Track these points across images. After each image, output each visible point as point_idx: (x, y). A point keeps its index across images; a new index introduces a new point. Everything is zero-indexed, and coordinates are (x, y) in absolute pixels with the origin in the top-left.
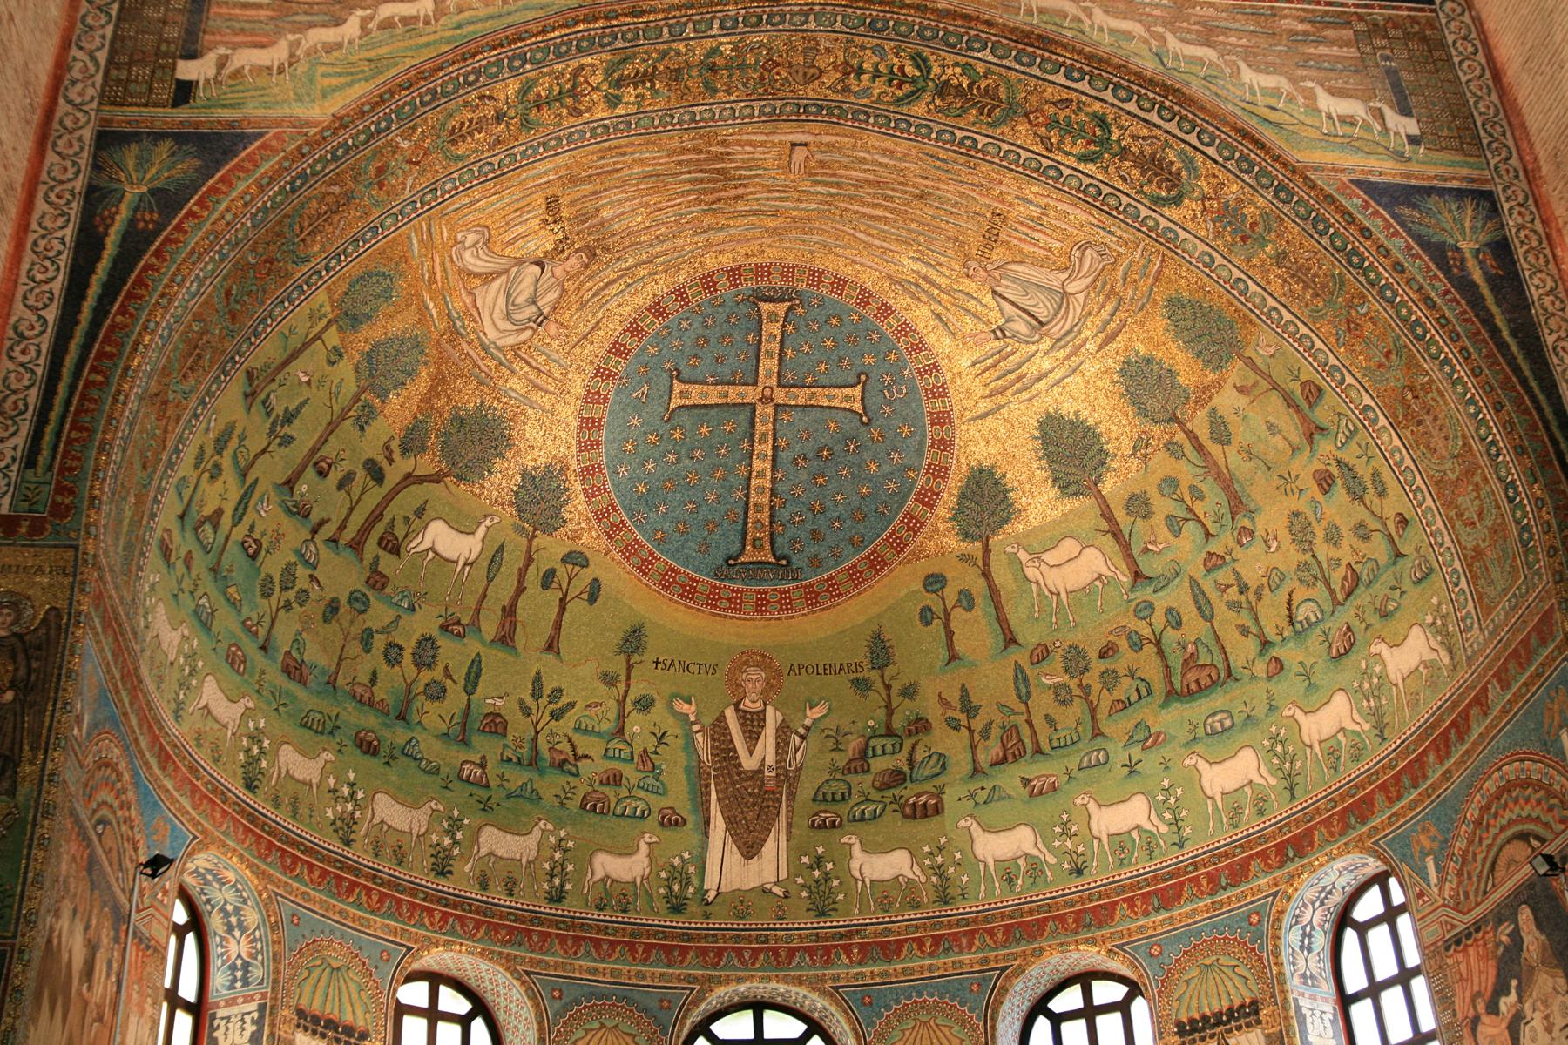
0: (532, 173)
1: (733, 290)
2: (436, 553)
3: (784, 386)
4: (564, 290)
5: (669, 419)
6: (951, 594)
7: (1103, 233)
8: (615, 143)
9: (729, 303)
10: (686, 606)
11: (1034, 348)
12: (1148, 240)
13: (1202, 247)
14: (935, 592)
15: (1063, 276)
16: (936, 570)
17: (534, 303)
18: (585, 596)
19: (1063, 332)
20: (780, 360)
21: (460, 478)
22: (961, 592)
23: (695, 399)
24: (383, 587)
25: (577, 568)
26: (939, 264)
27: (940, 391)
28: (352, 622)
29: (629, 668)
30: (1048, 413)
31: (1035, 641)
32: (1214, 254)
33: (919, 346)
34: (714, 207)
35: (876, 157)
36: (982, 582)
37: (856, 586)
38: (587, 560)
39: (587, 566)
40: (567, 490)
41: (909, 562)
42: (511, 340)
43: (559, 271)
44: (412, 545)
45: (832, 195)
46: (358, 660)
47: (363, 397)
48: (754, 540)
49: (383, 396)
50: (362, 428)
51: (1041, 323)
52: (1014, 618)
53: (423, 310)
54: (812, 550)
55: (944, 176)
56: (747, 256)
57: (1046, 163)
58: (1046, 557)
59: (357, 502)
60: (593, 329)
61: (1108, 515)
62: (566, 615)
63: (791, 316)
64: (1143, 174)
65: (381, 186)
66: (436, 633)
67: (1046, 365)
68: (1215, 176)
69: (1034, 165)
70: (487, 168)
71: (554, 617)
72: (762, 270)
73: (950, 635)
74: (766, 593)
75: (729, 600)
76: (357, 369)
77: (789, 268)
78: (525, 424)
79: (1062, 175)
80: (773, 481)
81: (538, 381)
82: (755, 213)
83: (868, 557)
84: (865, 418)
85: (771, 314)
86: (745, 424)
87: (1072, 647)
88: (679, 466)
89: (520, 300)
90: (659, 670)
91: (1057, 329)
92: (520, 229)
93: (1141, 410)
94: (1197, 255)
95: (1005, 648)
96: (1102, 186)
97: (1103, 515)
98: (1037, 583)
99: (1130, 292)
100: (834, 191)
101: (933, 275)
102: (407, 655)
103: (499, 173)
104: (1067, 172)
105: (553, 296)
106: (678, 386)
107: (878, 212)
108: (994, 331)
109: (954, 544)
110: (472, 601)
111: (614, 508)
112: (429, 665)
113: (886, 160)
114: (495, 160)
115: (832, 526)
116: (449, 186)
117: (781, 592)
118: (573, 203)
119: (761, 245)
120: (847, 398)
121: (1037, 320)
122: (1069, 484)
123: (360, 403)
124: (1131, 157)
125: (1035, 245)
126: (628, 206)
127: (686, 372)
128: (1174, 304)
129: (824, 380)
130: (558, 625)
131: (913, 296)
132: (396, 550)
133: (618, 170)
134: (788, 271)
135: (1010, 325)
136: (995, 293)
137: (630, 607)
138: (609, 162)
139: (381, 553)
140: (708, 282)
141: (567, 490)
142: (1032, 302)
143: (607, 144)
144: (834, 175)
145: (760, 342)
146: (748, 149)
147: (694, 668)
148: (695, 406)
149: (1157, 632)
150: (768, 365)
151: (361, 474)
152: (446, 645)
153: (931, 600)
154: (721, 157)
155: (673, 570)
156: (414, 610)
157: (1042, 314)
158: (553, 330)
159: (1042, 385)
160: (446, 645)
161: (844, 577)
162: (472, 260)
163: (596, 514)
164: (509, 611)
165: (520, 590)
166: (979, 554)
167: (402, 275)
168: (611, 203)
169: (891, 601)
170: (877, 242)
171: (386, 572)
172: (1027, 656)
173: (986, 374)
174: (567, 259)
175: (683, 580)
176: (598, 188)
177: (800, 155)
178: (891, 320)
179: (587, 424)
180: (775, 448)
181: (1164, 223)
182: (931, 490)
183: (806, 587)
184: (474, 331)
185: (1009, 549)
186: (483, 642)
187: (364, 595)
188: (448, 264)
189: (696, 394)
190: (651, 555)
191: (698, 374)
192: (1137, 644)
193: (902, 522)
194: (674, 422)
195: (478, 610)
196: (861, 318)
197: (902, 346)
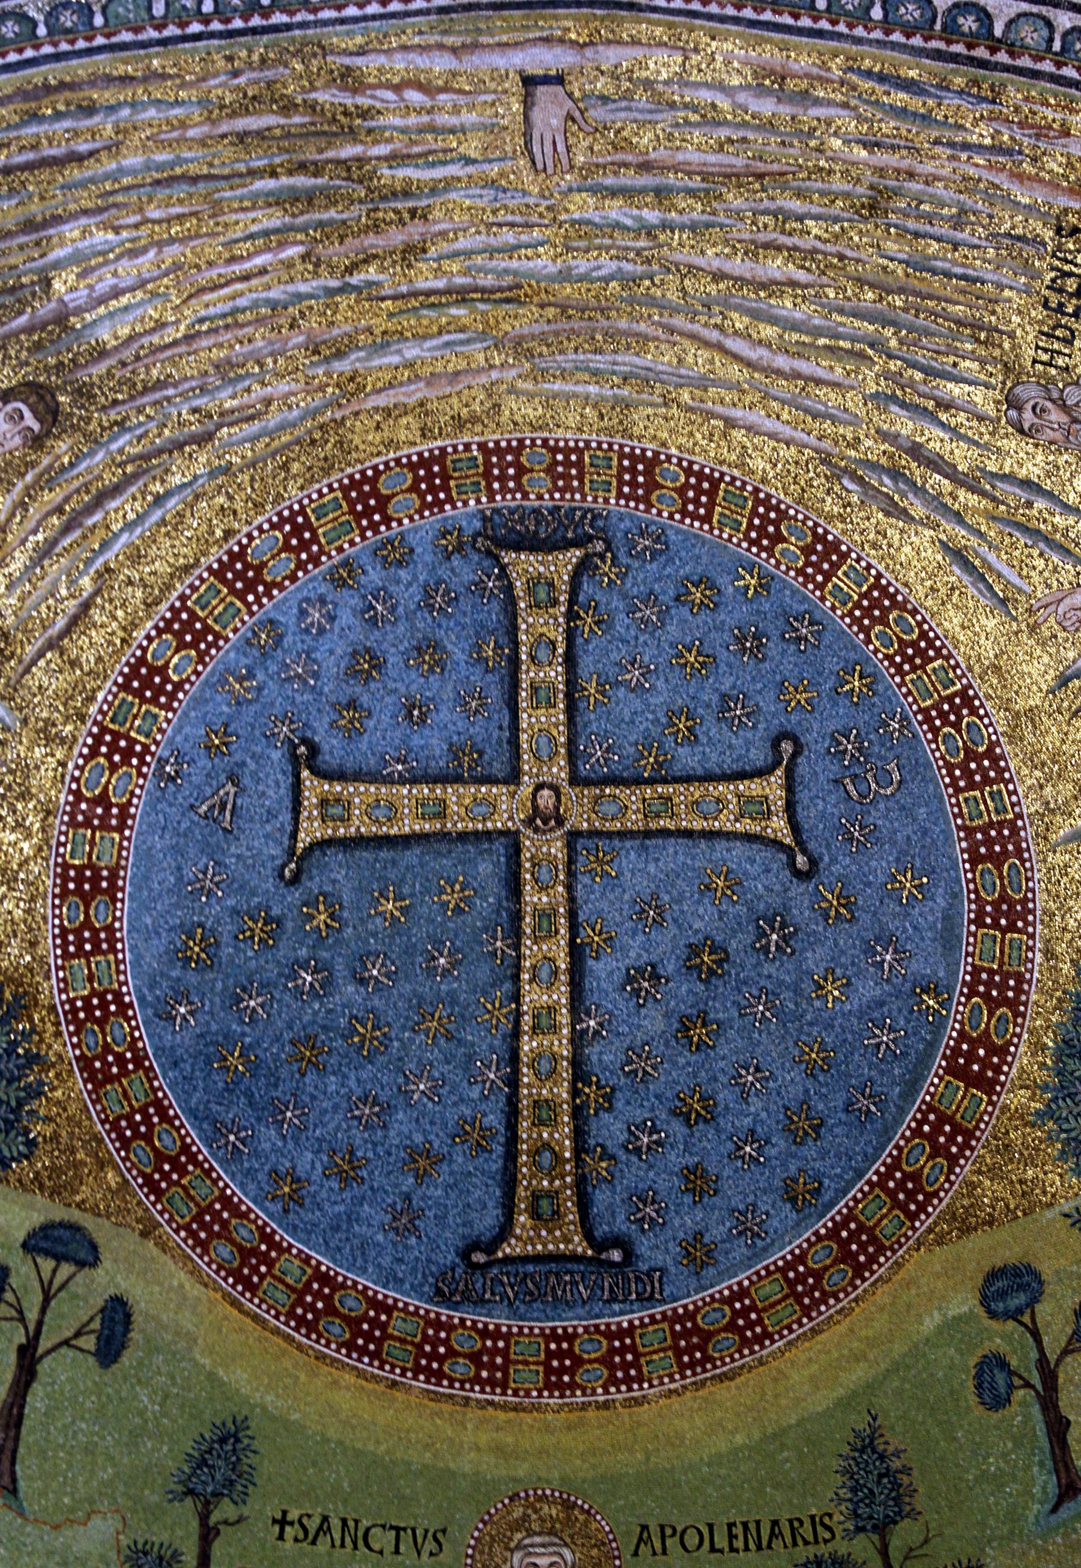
1: (431, 520)
3: (587, 782)
5: (295, 880)
8: (52, 73)
9: (424, 554)
10: (361, 1374)
14: (1015, 1315)
16: (1009, 1255)
18: (89, 1342)
20: (571, 710)
23: (360, 825)
25: (66, 1269)
26: (946, 405)
29: (208, 1535)
34: (355, 279)
35: (742, 97)
37: (806, 1311)
38: (94, 1248)
39: (94, 1261)
41: (940, 1241)
45: (650, 232)
48: (536, 1197)
55: (923, 138)
56: (460, 423)
60: (74, 621)
62: (37, 1388)
74: (571, 1338)
75: (475, 1358)
77: (567, 451)
80: (578, 1039)
82: (462, 295)
83: (833, 1233)
88: (331, 1003)
90: (289, 1544)
100: (652, 216)
101: (935, 440)
106: (313, 788)
107: (775, 267)
111: (162, 1112)
113: (767, 107)
115: (736, 1153)
117: (609, 1335)
119: (489, 390)
126: (128, 270)
129: (687, 758)
131: (893, 510)
133: (79, 159)
137: (211, 1376)
141: (33, 1059)
143: (36, 75)
144: (645, 167)
145: (514, 662)
146: (414, 96)
147: (382, 1539)
148: (359, 842)
155: (325, 1279)
161: (772, 1289)
163: (115, 1126)
168: (77, 258)
169: (899, 1349)
170: (782, 362)
175: (352, 1305)
176: (35, 208)
180: (576, 952)
183: (676, 1318)
190: (267, 1238)
193: (917, 1132)
194: (313, 884)
196: (766, 583)
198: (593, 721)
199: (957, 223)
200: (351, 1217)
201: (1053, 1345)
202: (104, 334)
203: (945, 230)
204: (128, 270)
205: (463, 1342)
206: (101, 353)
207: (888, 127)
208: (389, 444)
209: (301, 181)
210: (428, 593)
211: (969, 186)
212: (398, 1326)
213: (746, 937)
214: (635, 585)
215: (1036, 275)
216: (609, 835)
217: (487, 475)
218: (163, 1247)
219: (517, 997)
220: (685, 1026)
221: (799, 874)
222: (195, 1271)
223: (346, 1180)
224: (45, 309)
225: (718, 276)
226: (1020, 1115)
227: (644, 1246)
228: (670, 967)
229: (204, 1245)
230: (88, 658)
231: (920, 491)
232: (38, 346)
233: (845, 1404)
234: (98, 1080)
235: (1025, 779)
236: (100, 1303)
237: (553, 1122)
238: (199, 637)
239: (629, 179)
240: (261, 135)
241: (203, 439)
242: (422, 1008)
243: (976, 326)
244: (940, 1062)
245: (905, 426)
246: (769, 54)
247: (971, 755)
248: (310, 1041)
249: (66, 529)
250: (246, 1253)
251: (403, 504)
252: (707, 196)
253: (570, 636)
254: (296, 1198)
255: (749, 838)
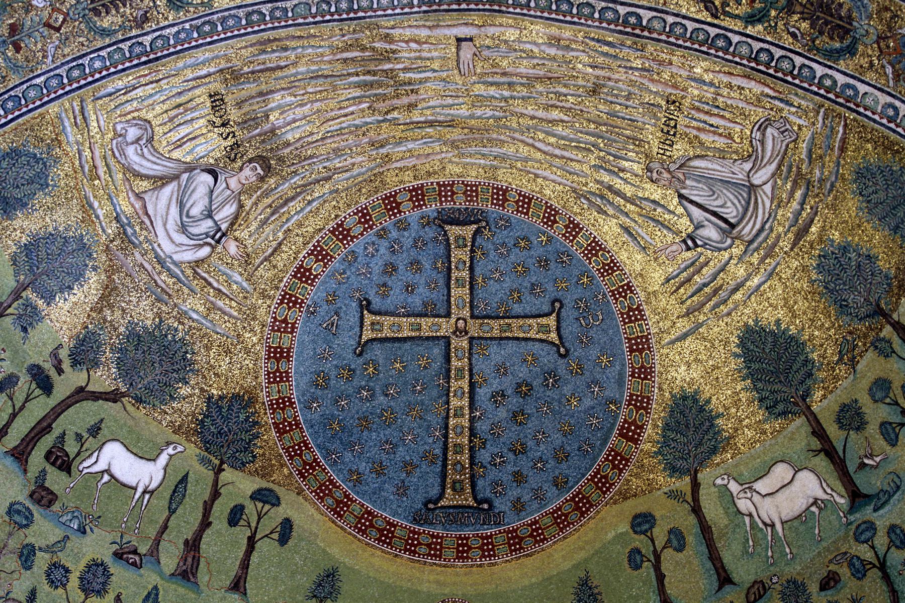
0: (190, 61)
1: (417, 213)
2: (112, 476)
3: (477, 318)
4: (241, 206)
5: (361, 354)
6: (660, 533)
7: (782, 105)
8: (271, 34)
9: (415, 226)
10: (383, 551)
11: (727, 255)
12: (827, 104)
13: (884, 99)
14: (644, 533)
15: (747, 166)
16: (642, 509)
17: (210, 216)
18: (275, 536)
19: (754, 232)
20: (472, 288)
21: (139, 400)
22: (670, 532)
23: (387, 333)
24: (50, 503)
25: (267, 507)
26: (623, 170)
27: (635, 314)
28: (10, 534)
30: (746, 325)
31: (752, 578)
32: (898, 103)
33: (612, 267)
34: (389, 117)
35: (543, 48)
36: (692, 519)
37: (561, 530)
38: (278, 499)
39: (279, 504)
40: (256, 423)
42: (189, 256)
43: (233, 183)
44: (85, 464)
46: (16, 575)
47: (24, 294)
48: (454, 482)
49: (49, 299)
50: (25, 330)
51: (733, 226)
52: (727, 558)
53: (87, 207)
54: (514, 493)
55: (615, 64)
56: (429, 174)
57: (713, 31)
58: (759, 486)
59: (22, 408)
60: (275, 250)
61: (819, 432)
62: (255, 554)
63: (479, 240)
64: (812, 26)
65: (18, 49)
66: (108, 559)
67: (741, 272)
68: (887, 9)
69: (701, 37)
70: (138, 50)
71: (241, 554)
72: (446, 190)
73: (661, 578)
74: (467, 539)
75: (428, 545)
76: (14, 260)
77: (472, 186)
78: (208, 348)
79: (730, 43)
80: (472, 420)
81: (220, 303)
82: (431, 124)
83: (573, 499)
84: (562, 350)
85: (457, 238)
86: (440, 361)
87: (792, 582)
88: (374, 403)
89: (195, 211)
91: (747, 230)
92: (184, 131)
93: (843, 307)
94: (879, 109)
95: (720, 588)
96: (773, 49)
97: (814, 433)
98: (750, 515)
99: (817, 172)
100: (506, 93)
101: (618, 184)
102: (74, 581)
103: (152, 56)
104: (735, 39)
105: (229, 210)
106: (368, 318)
107: (555, 114)
108: (684, 241)
109: (661, 479)
110: (152, 532)
111: (306, 445)
112: (98, 592)
113: (553, 51)
114: (146, 40)
115: (534, 467)
116: (98, 64)
117: (482, 538)
118: (239, 104)
119: (441, 161)
120: (546, 329)
121: (725, 221)
122: (776, 403)
123: (20, 301)
124: (798, 8)
125: (714, 133)
126: (299, 112)
127: (377, 303)
128: (862, 175)
129: (517, 309)
130: (245, 565)
131: (601, 211)
132: (66, 466)
133: (281, 68)
134: (472, 190)
135: (700, 232)
136: (681, 196)
137: (324, 551)
138: (272, 58)
139: (50, 469)
140: (391, 204)
141: (256, 423)
142: (719, 202)
143: (265, 35)
144: (504, 74)
146: (413, 45)
149: (881, 550)
150: (460, 293)
151: (24, 382)
152: (120, 574)
153: (639, 542)
154: (387, 56)
155: (369, 513)
156: (84, 532)
157: (731, 213)
158: (232, 248)
159: (738, 296)
160: (120, 574)
161: (548, 520)
162: (137, 159)
163: (287, 451)
164: (193, 546)
165: (205, 524)
166: (688, 490)
167: (57, 160)
168: (279, 107)
169: (598, 545)
170: (557, 152)
171: (55, 488)
172: (743, 595)
173: (682, 290)
174: (241, 169)
175: (380, 524)
176: (263, 87)
177: (467, 52)
178: (579, 239)
179: (278, 354)
180: (472, 385)
181: (841, 79)
182: (634, 423)
183: (509, 532)
184: (147, 240)
185: (719, 481)
186: (161, 574)
187: (28, 509)
188: (112, 162)
189: (388, 326)
190: (347, 496)
191: (389, 304)
192: (860, 570)
193: (607, 459)
194: (367, 356)
195: (157, 542)
196: (550, 239)
197: (593, 267)
198: (480, 293)
199: (628, 98)
200: (381, 489)
201: (659, 545)
202: (290, 137)
203: (623, 101)
204: (299, 112)
205: (424, 539)
206: (288, 144)
207: (600, 60)
208: (401, 182)
209: (368, 78)
210: (415, 241)
211: (632, 83)
212: (398, 532)
213: (540, 380)
214: (498, 239)
215: (659, 119)
216: (486, 339)
217: (440, 195)
218: (306, 499)
219: (448, 403)
220: (515, 415)
221: (561, 356)
222: (318, 509)
223: (379, 474)
224: (267, 127)
225: (533, 118)
226: (648, 453)
227: (497, 503)
228: (509, 392)
229: (322, 498)
230: (280, 265)
231: (611, 204)
232: (263, 141)
233: (576, 567)
234: (281, 432)
235: (652, 319)
236: (280, 520)
237: (462, 453)
238: (324, 257)
239: (498, 78)
240: (353, 59)
241: (328, 179)
242: (410, 406)
243: (635, 139)
244: (616, 431)
245: (606, 178)
246: (554, 31)
247: (630, 309)
248: (365, 418)
249: (273, 214)
250: (338, 502)
251: (406, 206)
252: (529, 86)
253: (472, 259)
254: (359, 481)
255: (542, 341)
